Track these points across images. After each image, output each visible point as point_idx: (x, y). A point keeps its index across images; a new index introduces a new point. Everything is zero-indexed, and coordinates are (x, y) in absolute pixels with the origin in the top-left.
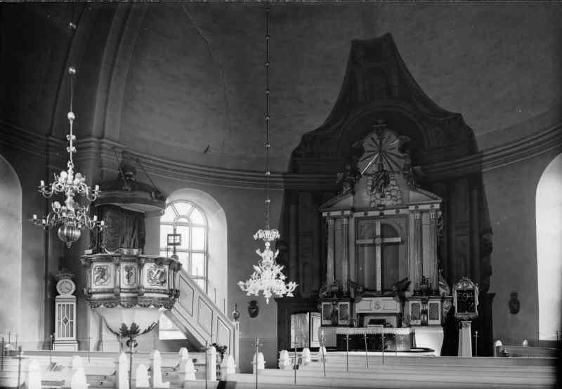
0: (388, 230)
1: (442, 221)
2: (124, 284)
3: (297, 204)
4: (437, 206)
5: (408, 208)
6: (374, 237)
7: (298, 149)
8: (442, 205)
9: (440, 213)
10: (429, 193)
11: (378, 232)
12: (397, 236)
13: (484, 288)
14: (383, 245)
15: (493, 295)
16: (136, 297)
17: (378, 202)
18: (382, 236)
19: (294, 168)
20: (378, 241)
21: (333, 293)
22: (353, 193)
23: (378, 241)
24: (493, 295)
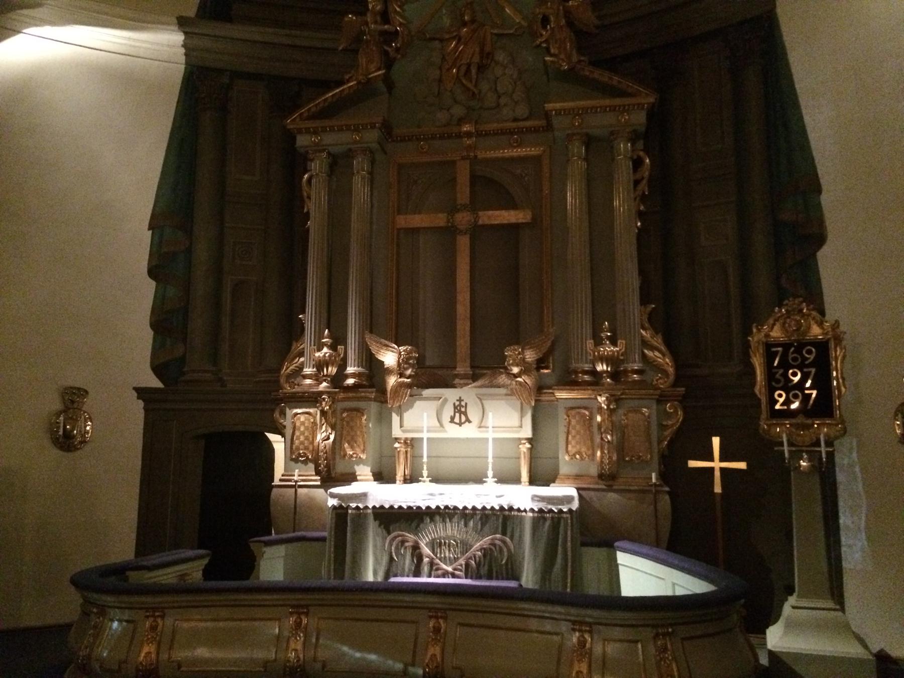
4: (640, 118)
8: (651, 115)
11: (463, 194)
23: (463, 219)
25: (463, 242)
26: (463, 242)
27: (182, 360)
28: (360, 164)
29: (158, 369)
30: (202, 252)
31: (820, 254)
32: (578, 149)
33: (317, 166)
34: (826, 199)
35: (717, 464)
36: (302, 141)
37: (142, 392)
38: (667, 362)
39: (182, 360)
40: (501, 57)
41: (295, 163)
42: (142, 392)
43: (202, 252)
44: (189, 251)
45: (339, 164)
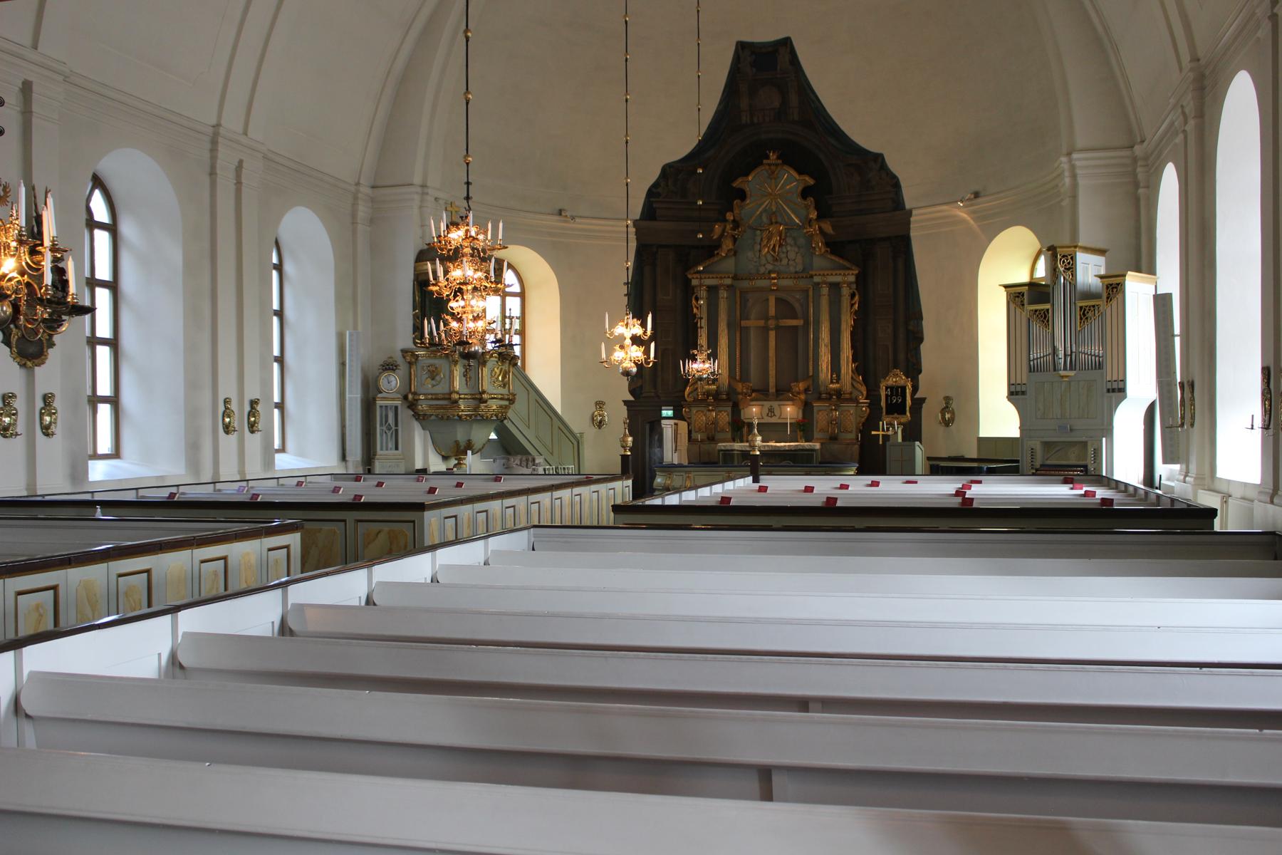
0: (785, 308)
1: (857, 298)
4: (852, 279)
5: (812, 277)
6: (767, 318)
8: (857, 276)
9: (854, 286)
10: (837, 259)
11: (772, 311)
12: (795, 317)
13: (915, 389)
14: (778, 328)
15: (923, 400)
16: (506, 407)
17: (770, 267)
18: (777, 318)
19: (650, 212)
20: (772, 323)
21: (708, 394)
22: (735, 254)
23: (772, 323)
24: (923, 400)
25: (772, 334)
26: (772, 334)
28: (723, 294)
29: (632, 392)
31: (922, 346)
32: (825, 290)
34: (924, 323)
35: (881, 433)
36: (695, 282)
37: (626, 402)
38: (863, 389)
40: (789, 240)
41: (688, 292)
42: (626, 402)
45: (712, 290)
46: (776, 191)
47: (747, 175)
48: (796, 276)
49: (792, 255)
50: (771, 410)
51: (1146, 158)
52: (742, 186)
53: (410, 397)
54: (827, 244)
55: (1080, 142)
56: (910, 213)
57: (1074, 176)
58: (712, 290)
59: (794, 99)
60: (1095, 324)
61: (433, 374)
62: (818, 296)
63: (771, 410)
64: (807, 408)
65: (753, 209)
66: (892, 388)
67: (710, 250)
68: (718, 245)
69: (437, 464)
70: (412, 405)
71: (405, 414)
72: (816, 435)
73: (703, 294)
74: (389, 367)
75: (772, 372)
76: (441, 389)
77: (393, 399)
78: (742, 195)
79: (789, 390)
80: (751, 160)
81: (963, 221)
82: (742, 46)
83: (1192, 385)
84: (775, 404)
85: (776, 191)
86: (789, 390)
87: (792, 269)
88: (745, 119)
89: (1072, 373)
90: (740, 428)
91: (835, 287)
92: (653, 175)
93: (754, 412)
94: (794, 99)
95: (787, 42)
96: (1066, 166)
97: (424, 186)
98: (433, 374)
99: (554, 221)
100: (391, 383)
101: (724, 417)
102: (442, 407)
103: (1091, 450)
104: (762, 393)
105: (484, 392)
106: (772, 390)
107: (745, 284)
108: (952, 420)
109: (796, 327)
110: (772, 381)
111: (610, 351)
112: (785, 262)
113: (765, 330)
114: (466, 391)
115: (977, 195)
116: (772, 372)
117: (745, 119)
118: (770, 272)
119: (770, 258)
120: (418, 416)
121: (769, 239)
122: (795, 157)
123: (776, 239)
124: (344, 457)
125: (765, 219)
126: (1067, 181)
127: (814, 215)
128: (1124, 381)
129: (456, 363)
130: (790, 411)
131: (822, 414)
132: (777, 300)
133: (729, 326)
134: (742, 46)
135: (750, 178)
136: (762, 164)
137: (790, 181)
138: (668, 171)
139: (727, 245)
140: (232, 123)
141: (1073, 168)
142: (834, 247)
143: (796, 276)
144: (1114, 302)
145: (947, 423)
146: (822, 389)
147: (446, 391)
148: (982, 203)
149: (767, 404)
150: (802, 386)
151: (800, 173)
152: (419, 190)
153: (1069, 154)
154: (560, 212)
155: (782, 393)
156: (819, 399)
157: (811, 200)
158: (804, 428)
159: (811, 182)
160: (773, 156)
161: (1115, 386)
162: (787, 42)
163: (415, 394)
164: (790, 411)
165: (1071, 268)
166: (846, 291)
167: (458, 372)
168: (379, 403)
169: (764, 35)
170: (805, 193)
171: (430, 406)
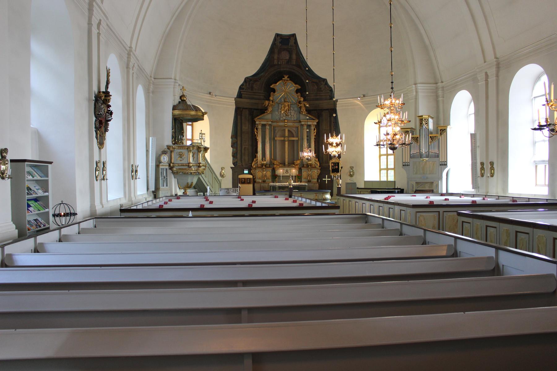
0: (291, 134)
2: (191, 160)
3: (241, 115)
4: (315, 123)
7: (242, 85)
11: (287, 134)
12: (294, 137)
14: (289, 141)
17: (284, 118)
18: (288, 137)
19: (240, 95)
21: (262, 165)
25: (287, 143)
26: (287, 143)
27: (237, 162)
28: (268, 127)
29: (234, 164)
30: (239, 142)
33: (260, 127)
36: (257, 122)
37: (231, 168)
38: (318, 164)
39: (237, 162)
40: (292, 108)
42: (231, 168)
43: (239, 142)
44: (237, 142)
46: (285, 90)
47: (276, 83)
48: (294, 122)
49: (292, 114)
50: (287, 171)
51: (443, 88)
52: (274, 87)
53: (171, 165)
54: (306, 110)
55: (419, 80)
56: (337, 101)
57: (417, 92)
58: (264, 126)
59: (294, 57)
60: (436, 143)
61: (181, 155)
62: (302, 129)
63: (287, 171)
64: (300, 170)
65: (278, 96)
66: (334, 163)
67: (263, 111)
68: (266, 109)
69: (180, 192)
70: (171, 168)
71: (169, 171)
72: (303, 180)
73: (260, 127)
74: (164, 152)
75: (287, 157)
76: (184, 162)
77: (166, 166)
78: (274, 91)
79: (294, 163)
80: (278, 77)
81: (358, 105)
82: (277, 35)
83: (492, 164)
84: (288, 169)
85: (285, 90)
86: (294, 163)
87: (293, 119)
88: (276, 62)
89: (427, 159)
90: (275, 177)
91: (309, 126)
92: (242, 81)
93: (280, 171)
94: (294, 57)
95: (294, 35)
96: (414, 88)
97: (175, 80)
98: (181, 155)
99: (208, 97)
100: (165, 159)
101: (269, 173)
102: (185, 169)
103: (434, 184)
104: (283, 164)
105: (200, 163)
106: (286, 163)
107: (275, 124)
108: (353, 174)
109: (294, 141)
110: (287, 160)
111: (326, 148)
112: (290, 116)
113: (284, 141)
114: (193, 163)
115: (364, 96)
116: (287, 157)
117: (276, 62)
118: (284, 120)
119: (284, 115)
120: (173, 173)
121: (284, 108)
122: (295, 78)
123: (287, 108)
124: (148, 189)
125: (282, 100)
126: (414, 93)
127: (302, 99)
128: (446, 162)
129: (190, 151)
130: (294, 171)
131: (305, 173)
132: (289, 131)
133: (270, 139)
134: (277, 35)
135: (278, 84)
136: (282, 79)
137: (292, 87)
138: (247, 80)
139: (270, 109)
140: (133, 46)
141: (416, 89)
142: (309, 111)
143: (294, 122)
144: (443, 135)
145: (351, 176)
146: (305, 163)
147: (187, 162)
148: (366, 99)
149: (286, 169)
150: (298, 162)
151: (295, 84)
152: (173, 80)
153: (415, 84)
154: (210, 93)
155: (291, 164)
156: (303, 167)
157: (299, 94)
158: (298, 178)
159: (300, 87)
160: (286, 77)
161: (443, 163)
162: (294, 35)
163: (173, 163)
164: (294, 171)
165: (427, 123)
166: (313, 128)
167: (191, 155)
168: (161, 167)
169: (286, 32)
170: (297, 91)
171: (180, 169)
